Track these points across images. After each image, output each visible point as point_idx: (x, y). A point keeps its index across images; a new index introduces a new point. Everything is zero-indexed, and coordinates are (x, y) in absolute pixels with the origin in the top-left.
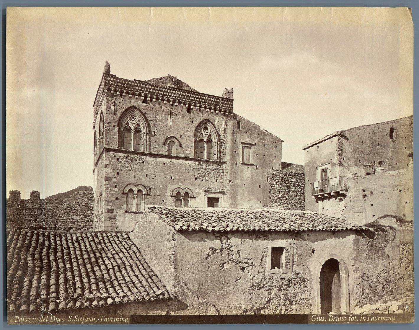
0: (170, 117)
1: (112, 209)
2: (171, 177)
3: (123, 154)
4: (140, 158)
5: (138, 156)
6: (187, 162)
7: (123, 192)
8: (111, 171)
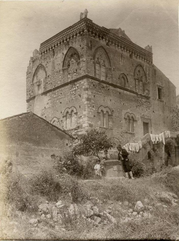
0: (122, 59)
1: (92, 124)
2: (124, 104)
3: (97, 82)
4: (107, 86)
5: (106, 85)
6: (132, 94)
7: (98, 111)
8: (91, 94)
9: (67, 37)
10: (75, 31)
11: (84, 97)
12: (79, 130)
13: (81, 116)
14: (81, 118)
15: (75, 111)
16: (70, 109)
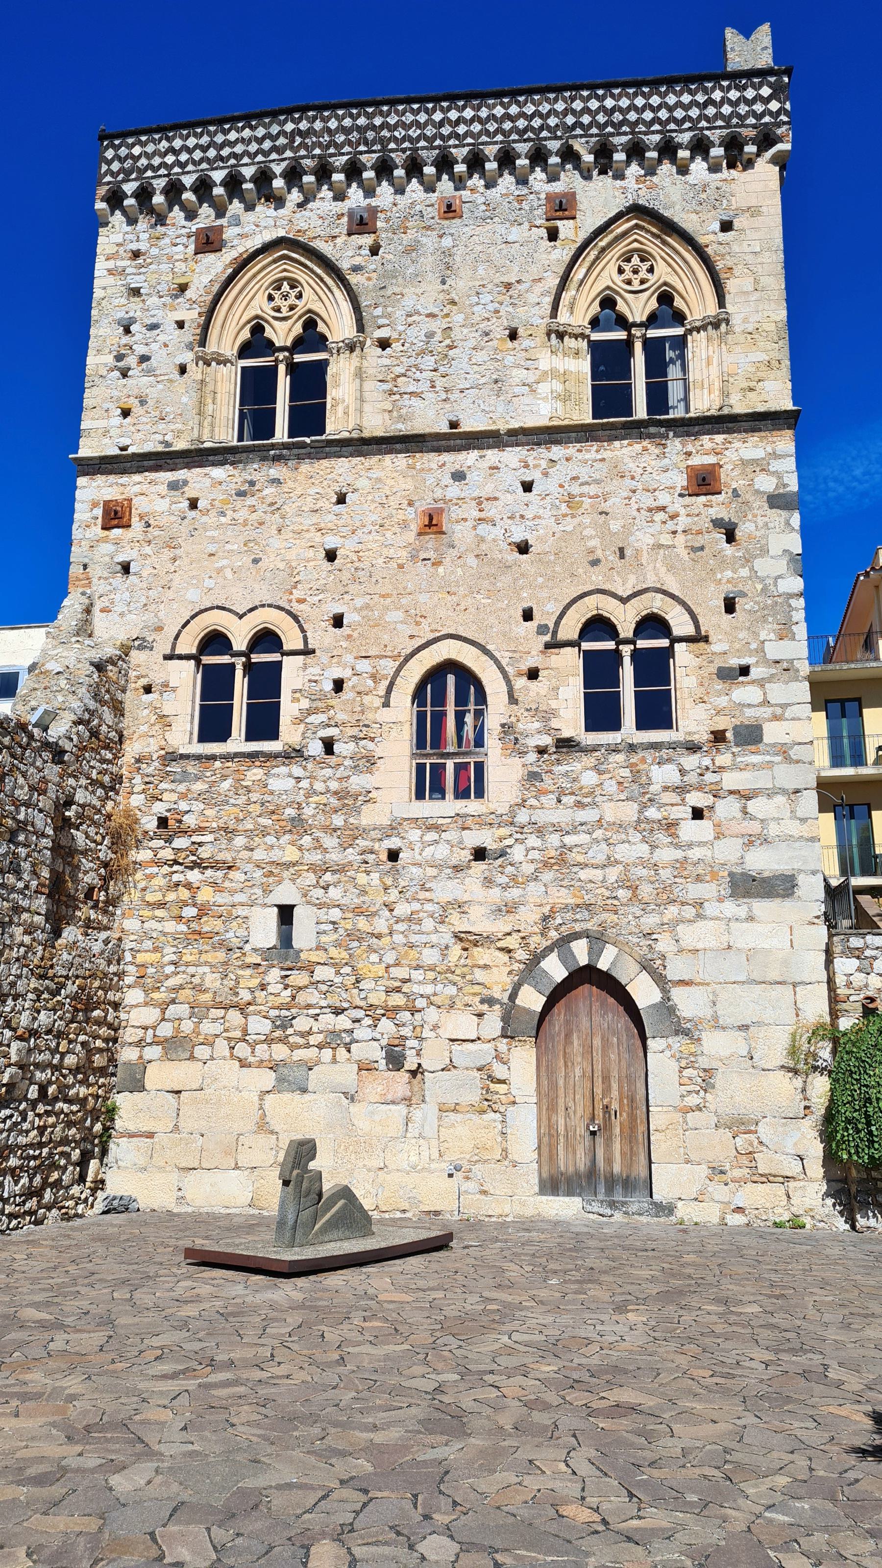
9: (612, 135)
10: (687, 125)
11: (775, 548)
12: (723, 759)
13: (745, 671)
14: (741, 679)
15: (681, 625)
16: (624, 600)
